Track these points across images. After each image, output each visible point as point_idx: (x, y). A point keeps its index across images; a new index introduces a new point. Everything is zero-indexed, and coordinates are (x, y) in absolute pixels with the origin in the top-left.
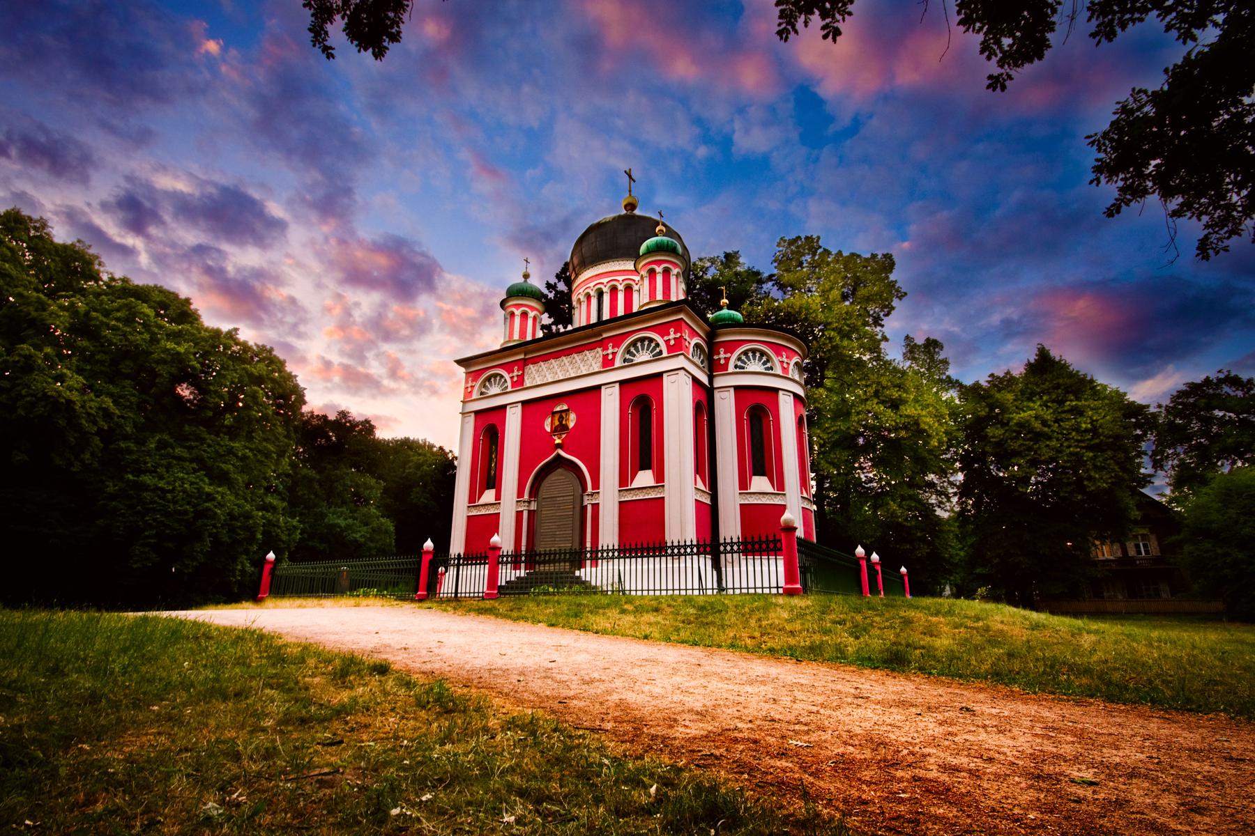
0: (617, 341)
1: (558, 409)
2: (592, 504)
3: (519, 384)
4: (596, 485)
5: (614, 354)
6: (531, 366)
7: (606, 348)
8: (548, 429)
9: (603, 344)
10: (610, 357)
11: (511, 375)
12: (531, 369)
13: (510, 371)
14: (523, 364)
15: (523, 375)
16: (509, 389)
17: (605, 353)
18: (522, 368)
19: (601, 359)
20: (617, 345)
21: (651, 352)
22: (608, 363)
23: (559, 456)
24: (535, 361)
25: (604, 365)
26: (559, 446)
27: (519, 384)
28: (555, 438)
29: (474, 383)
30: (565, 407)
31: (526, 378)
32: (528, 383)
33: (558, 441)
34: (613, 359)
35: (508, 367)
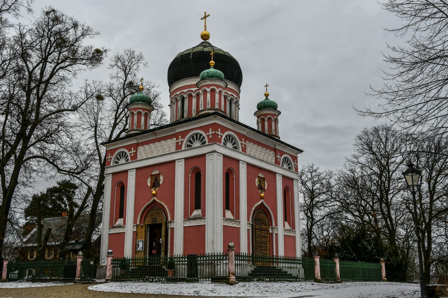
0: (184, 134)
1: (154, 173)
2: (171, 228)
3: (134, 158)
4: (173, 218)
5: (182, 142)
6: (141, 147)
7: (178, 139)
8: (149, 185)
9: (176, 136)
10: (180, 144)
11: (130, 152)
12: (141, 149)
13: (129, 150)
14: (137, 146)
15: (136, 152)
16: (130, 161)
17: (177, 141)
18: (136, 149)
19: (175, 145)
20: (183, 137)
21: (201, 141)
22: (178, 147)
23: (154, 201)
24: (143, 144)
25: (177, 148)
26: (154, 195)
27: (134, 158)
28: (153, 190)
29: (112, 156)
30: (158, 172)
31: (138, 154)
32: (139, 158)
33: (154, 192)
34: (181, 145)
35: (129, 147)
